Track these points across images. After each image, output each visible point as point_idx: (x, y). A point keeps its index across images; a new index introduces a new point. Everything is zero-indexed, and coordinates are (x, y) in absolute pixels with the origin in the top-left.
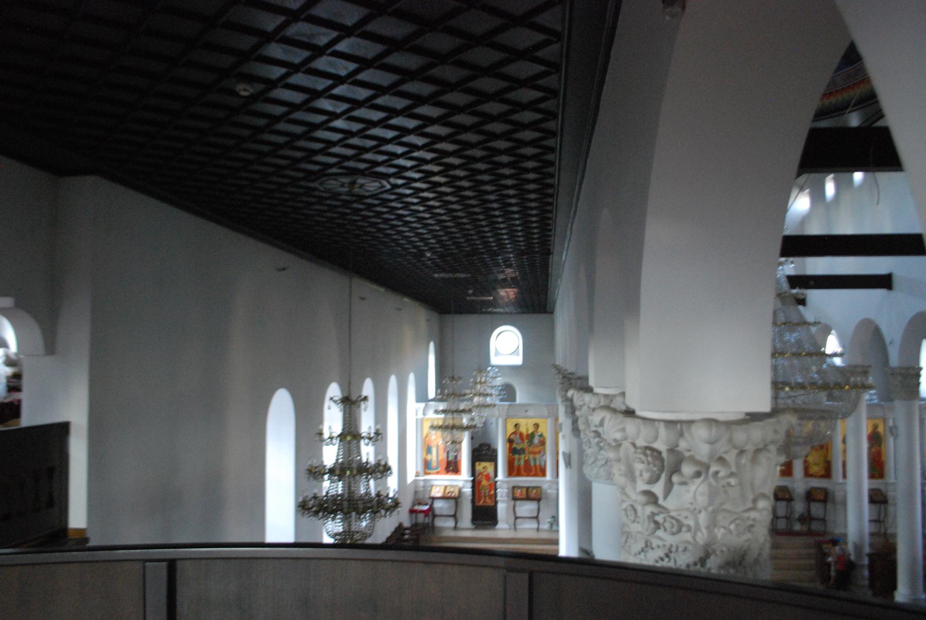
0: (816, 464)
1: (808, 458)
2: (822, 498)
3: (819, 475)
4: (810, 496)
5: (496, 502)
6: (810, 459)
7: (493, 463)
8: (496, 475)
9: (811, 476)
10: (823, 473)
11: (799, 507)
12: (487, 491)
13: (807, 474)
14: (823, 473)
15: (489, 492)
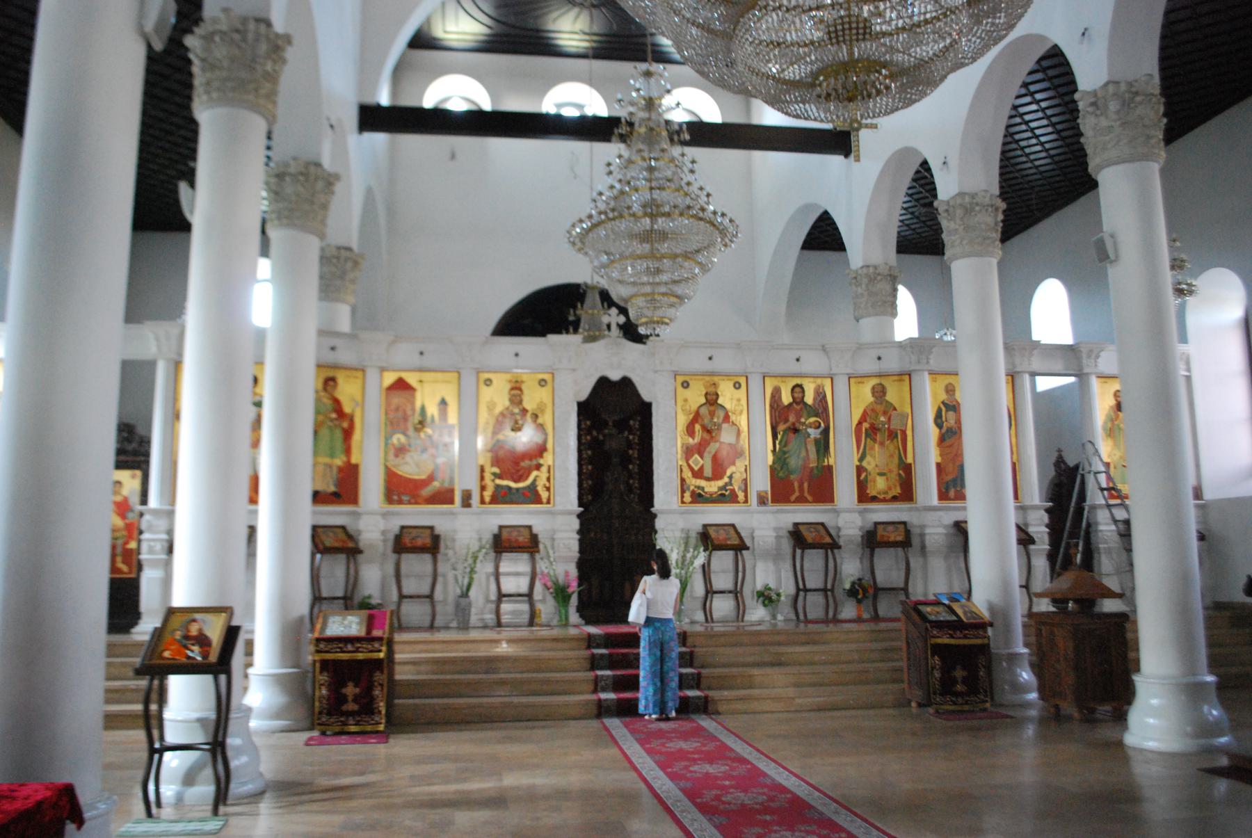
0: (881, 474)
1: (864, 464)
2: (900, 538)
3: (889, 496)
4: (872, 540)
5: (140, 567)
6: (869, 464)
7: (138, 473)
8: (144, 499)
9: (874, 499)
10: (897, 491)
11: (851, 568)
12: (120, 542)
13: (864, 496)
14: (897, 491)
15: (126, 543)
